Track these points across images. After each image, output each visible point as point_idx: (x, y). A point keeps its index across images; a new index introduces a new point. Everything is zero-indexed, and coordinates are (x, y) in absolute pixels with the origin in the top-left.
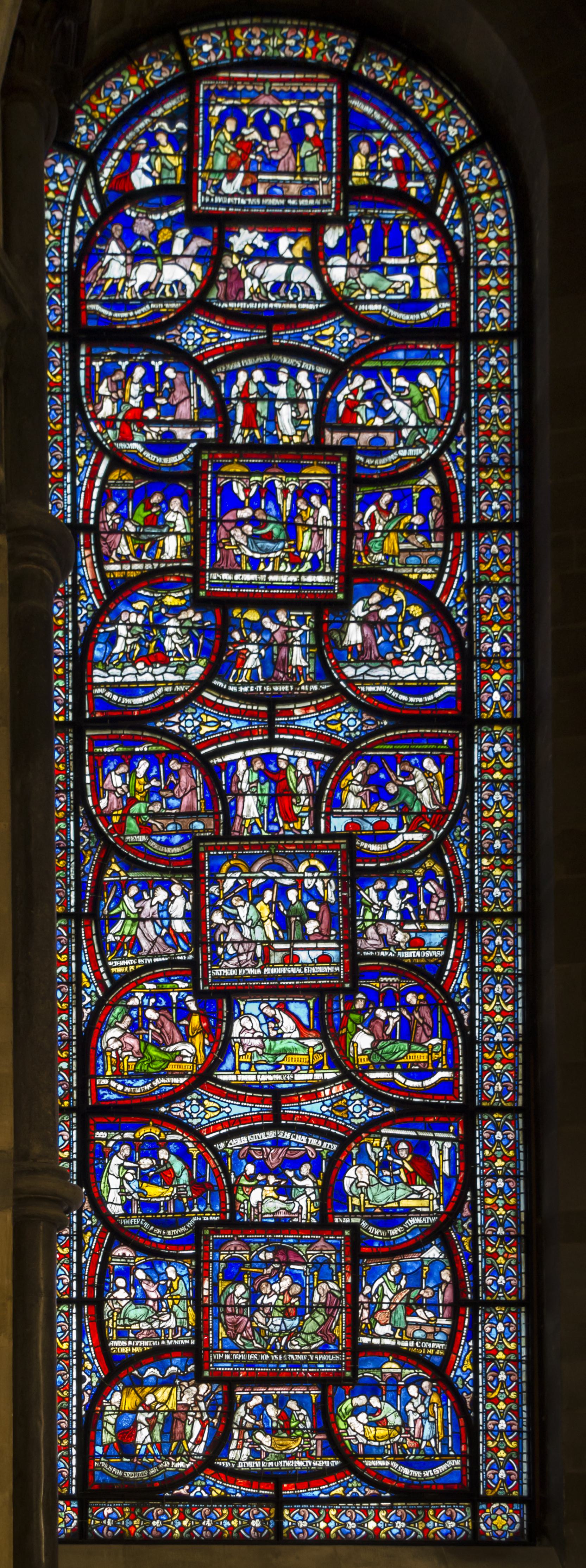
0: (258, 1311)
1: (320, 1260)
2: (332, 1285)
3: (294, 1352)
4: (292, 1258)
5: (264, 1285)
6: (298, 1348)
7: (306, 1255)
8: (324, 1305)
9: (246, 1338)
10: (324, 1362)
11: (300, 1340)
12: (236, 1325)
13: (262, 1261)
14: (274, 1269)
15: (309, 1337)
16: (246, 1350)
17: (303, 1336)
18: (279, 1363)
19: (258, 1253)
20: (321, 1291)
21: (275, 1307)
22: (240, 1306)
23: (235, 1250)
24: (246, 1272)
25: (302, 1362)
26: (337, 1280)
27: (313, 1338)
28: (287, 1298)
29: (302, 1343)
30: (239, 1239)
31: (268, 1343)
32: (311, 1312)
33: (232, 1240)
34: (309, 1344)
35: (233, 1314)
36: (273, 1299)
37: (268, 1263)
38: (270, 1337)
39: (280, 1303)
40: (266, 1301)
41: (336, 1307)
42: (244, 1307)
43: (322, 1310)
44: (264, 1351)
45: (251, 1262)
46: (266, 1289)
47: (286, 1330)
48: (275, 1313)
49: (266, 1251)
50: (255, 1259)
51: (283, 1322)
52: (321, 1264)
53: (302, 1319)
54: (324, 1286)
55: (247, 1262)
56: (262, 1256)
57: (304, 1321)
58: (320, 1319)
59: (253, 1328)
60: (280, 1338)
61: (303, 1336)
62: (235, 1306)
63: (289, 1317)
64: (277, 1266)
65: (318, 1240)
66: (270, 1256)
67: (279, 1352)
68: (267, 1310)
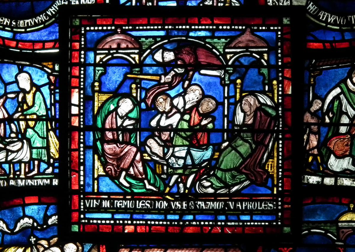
0: (152, 137)
1: (245, 61)
2: (264, 99)
3: (206, 197)
4: (203, 59)
5: (160, 99)
6: (210, 191)
7: (224, 54)
8: (250, 128)
9: (134, 177)
10: (251, 213)
11: (213, 180)
12: (119, 158)
13: (158, 64)
14: (177, 75)
15: (228, 176)
16: (133, 194)
17: (219, 174)
18: (182, 213)
19: (152, 53)
20: (246, 108)
21: (177, 131)
22: (124, 130)
23: (119, 48)
24: (134, 81)
25: (216, 212)
26: (271, 90)
27: (233, 177)
28: (196, 118)
29: (217, 184)
30: (124, 32)
31: (166, 185)
32: (231, 139)
33: (115, 32)
34: (228, 186)
35: (115, 141)
36: (174, 120)
37: (166, 66)
38: (170, 176)
39: (185, 125)
40: (164, 122)
41: (269, 131)
42: (131, 131)
43: (247, 136)
44: (161, 195)
45: (141, 64)
46: (163, 105)
47: (194, 165)
48: (178, 141)
49: (165, 50)
50: (148, 61)
51: (189, 153)
52: (248, 68)
53: (217, 148)
54: (251, 99)
55: (136, 66)
56: (158, 56)
57: (221, 151)
58: (244, 148)
59: (145, 162)
60: (183, 178)
61: (219, 174)
62: (118, 129)
63: (200, 147)
64: (180, 71)
65: (243, 32)
66: (170, 56)
67: (182, 197)
68: (165, 136)
